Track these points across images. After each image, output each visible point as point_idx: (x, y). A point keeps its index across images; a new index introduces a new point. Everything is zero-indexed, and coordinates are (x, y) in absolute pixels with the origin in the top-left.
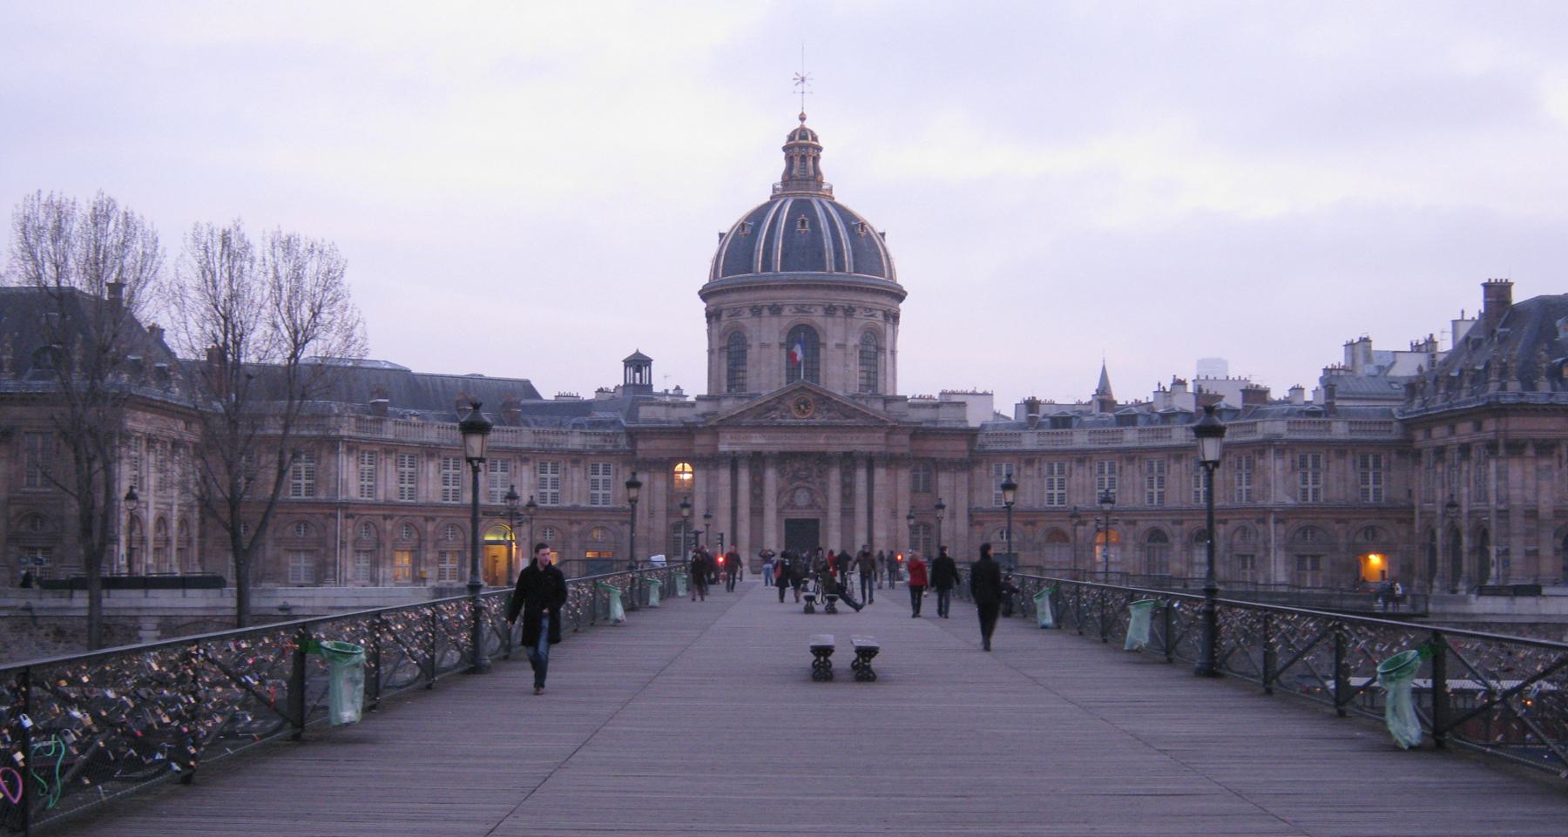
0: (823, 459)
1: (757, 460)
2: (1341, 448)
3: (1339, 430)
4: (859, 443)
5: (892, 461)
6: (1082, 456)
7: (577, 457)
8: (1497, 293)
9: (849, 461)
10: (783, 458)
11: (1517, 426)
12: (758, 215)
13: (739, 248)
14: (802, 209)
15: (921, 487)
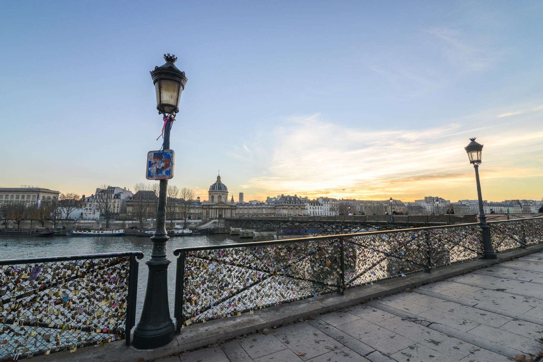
0: (223, 208)
1: (216, 209)
2: (269, 208)
3: (269, 207)
4: (226, 207)
5: (229, 209)
6: (246, 208)
7: (197, 208)
8: (283, 195)
9: (225, 209)
10: (219, 208)
11: (284, 207)
12: (215, 184)
13: (213, 188)
14: (219, 184)
15: (231, 211)
